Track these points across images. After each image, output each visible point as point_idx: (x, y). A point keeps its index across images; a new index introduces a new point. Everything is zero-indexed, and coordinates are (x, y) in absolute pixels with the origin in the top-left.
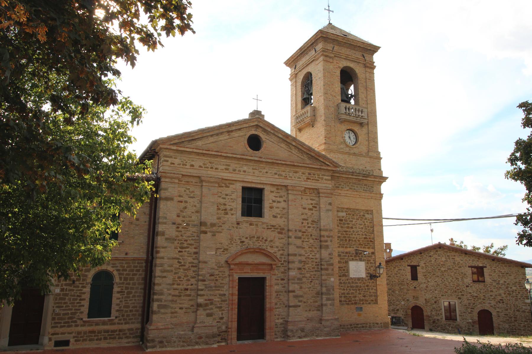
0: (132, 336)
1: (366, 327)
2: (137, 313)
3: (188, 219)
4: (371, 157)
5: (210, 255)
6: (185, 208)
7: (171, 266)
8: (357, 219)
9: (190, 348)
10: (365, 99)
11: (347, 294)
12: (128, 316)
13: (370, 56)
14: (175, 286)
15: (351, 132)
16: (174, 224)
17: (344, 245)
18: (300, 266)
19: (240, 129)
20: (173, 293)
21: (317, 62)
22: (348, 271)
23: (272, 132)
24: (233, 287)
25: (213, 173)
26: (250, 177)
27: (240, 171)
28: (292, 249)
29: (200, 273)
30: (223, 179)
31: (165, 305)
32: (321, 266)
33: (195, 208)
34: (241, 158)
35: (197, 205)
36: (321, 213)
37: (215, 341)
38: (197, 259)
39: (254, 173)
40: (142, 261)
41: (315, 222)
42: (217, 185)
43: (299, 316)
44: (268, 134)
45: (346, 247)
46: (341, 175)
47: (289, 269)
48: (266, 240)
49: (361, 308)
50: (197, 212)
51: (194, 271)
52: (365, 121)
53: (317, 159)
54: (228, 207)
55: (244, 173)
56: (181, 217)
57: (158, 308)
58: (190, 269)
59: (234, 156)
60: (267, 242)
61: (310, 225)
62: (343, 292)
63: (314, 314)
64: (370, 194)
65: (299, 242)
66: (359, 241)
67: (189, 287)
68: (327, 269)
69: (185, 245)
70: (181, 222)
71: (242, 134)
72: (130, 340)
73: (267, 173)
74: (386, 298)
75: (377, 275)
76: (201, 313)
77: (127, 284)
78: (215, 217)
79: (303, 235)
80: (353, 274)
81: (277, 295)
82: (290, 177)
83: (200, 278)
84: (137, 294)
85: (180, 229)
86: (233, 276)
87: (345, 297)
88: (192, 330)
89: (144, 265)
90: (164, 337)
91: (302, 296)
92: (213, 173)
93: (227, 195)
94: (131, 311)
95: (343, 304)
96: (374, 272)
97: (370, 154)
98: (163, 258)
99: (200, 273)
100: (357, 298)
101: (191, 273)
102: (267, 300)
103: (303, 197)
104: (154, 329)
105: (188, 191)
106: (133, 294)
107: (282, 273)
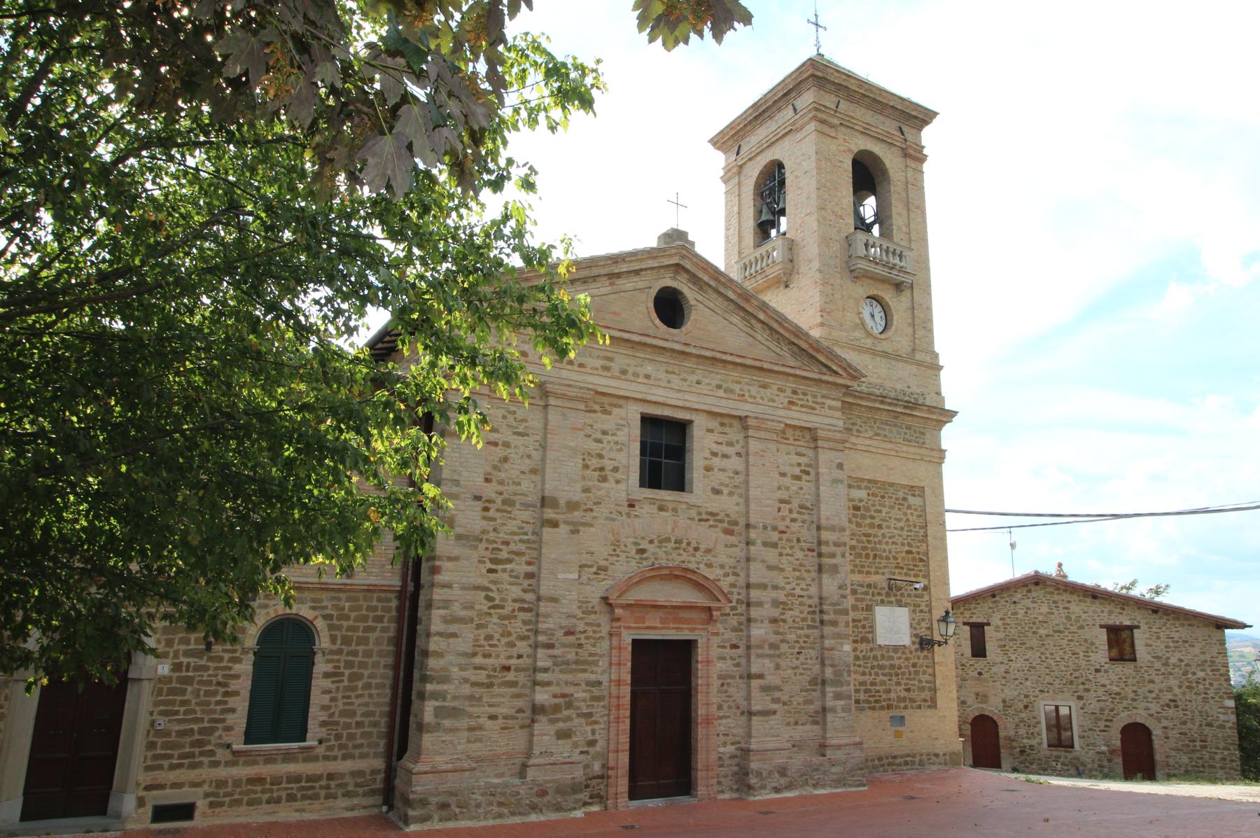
0: (360, 790)
1: (913, 763)
2: (375, 730)
3: (512, 488)
4: (919, 364)
5: (568, 585)
6: (506, 459)
7: (470, 607)
8: (892, 507)
9: (517, 820)
10: (904, 229)
11: (872, 684)
12: (351, 737)
13: (914, 131)
14: (479, 660)
15: (875, 303)
16: (478, 498)
17: (863, 566)
18: (776, 613)
19: (637, 272)
20: (473, 678)
21: (799, 136)
22: (872, 630)
23: (713, 283)
24: (619, 664)
25: (575, 376)
26: (660, 391)
27: (636, 375)
28: (757, 573)
29: (542, 626)
30: (597, 392)
31: (454, 709)
32: (819, 615)
33: (528, 461)
34: (640, 343)
35: (534, 454)
36: (822, 488)
37: (576, 801)
38: (533, 591)
39: (669, 382)
40: (389, 595)
41: (807, 508)
42: (583, 407)
43: (774, 737)
44: (701, 288)
45: (868, 573)
46: (859, 402)
47: (749, 620)
48: (696, 549)
49: (903, 717)
50: (534, 471)
51: (525, 622)
52: (907, 279)
53: (812, 357)
54: (608, 464)
55: (646, 381)
56: (494, 483)
57: (436, 716)
58: (515, 617)
59: (626, 336)
60: (698, 554)
61: (794, 515)
62: (862, 678)
63: (807, 731)
64: (917, 450)
65: (771, 555)
66: (895, 558)
67: (513, 661)
68: (834, 623)
69: (504, 555)
70: (494, 495)
71: (641, 285)
72: (356, 801)
73: (698, 383)
74: (954, 695)
75: (937, 638)
76: (543, 727)
77: (349, 654)
78: (578, 487)
79: (780, 539)
80: (883, 638)
81: (722, 685)
82: (751, 396)
83: (542, 638)
84: (374, 681)
85: (492, 513)
86: (619, 635)
87: (866, 691)
88: (522, 772)
89: (394, 604)
90: (451, 794)
91: (778, 689)
92: (575, 376)
93: (605, 433)
94: (358, 724)
95: (862, 709)
96: (928, 633)
97: (918, 356)
98: (448, 586)
99: (542, 626)
100: (892, 695)
101: (517, 627)
102: (700, 696)
103: (782, 447)
104: (425, 773)
105: (511, 418)
106: (365, 680)
107: (734, 630)
